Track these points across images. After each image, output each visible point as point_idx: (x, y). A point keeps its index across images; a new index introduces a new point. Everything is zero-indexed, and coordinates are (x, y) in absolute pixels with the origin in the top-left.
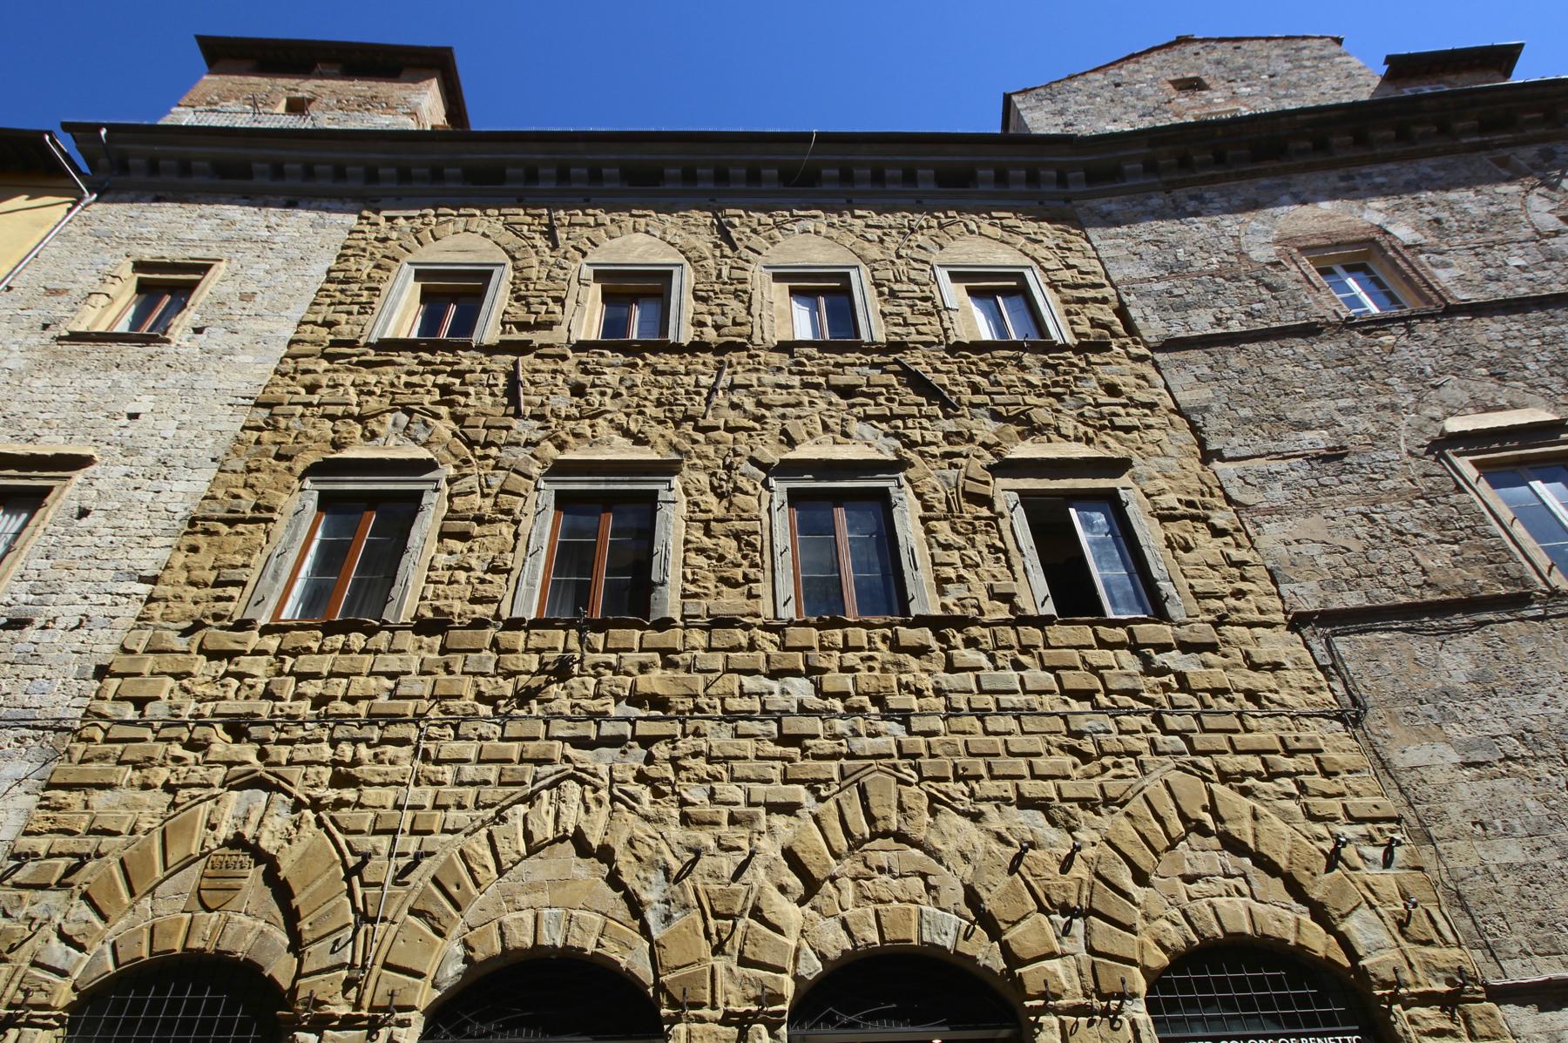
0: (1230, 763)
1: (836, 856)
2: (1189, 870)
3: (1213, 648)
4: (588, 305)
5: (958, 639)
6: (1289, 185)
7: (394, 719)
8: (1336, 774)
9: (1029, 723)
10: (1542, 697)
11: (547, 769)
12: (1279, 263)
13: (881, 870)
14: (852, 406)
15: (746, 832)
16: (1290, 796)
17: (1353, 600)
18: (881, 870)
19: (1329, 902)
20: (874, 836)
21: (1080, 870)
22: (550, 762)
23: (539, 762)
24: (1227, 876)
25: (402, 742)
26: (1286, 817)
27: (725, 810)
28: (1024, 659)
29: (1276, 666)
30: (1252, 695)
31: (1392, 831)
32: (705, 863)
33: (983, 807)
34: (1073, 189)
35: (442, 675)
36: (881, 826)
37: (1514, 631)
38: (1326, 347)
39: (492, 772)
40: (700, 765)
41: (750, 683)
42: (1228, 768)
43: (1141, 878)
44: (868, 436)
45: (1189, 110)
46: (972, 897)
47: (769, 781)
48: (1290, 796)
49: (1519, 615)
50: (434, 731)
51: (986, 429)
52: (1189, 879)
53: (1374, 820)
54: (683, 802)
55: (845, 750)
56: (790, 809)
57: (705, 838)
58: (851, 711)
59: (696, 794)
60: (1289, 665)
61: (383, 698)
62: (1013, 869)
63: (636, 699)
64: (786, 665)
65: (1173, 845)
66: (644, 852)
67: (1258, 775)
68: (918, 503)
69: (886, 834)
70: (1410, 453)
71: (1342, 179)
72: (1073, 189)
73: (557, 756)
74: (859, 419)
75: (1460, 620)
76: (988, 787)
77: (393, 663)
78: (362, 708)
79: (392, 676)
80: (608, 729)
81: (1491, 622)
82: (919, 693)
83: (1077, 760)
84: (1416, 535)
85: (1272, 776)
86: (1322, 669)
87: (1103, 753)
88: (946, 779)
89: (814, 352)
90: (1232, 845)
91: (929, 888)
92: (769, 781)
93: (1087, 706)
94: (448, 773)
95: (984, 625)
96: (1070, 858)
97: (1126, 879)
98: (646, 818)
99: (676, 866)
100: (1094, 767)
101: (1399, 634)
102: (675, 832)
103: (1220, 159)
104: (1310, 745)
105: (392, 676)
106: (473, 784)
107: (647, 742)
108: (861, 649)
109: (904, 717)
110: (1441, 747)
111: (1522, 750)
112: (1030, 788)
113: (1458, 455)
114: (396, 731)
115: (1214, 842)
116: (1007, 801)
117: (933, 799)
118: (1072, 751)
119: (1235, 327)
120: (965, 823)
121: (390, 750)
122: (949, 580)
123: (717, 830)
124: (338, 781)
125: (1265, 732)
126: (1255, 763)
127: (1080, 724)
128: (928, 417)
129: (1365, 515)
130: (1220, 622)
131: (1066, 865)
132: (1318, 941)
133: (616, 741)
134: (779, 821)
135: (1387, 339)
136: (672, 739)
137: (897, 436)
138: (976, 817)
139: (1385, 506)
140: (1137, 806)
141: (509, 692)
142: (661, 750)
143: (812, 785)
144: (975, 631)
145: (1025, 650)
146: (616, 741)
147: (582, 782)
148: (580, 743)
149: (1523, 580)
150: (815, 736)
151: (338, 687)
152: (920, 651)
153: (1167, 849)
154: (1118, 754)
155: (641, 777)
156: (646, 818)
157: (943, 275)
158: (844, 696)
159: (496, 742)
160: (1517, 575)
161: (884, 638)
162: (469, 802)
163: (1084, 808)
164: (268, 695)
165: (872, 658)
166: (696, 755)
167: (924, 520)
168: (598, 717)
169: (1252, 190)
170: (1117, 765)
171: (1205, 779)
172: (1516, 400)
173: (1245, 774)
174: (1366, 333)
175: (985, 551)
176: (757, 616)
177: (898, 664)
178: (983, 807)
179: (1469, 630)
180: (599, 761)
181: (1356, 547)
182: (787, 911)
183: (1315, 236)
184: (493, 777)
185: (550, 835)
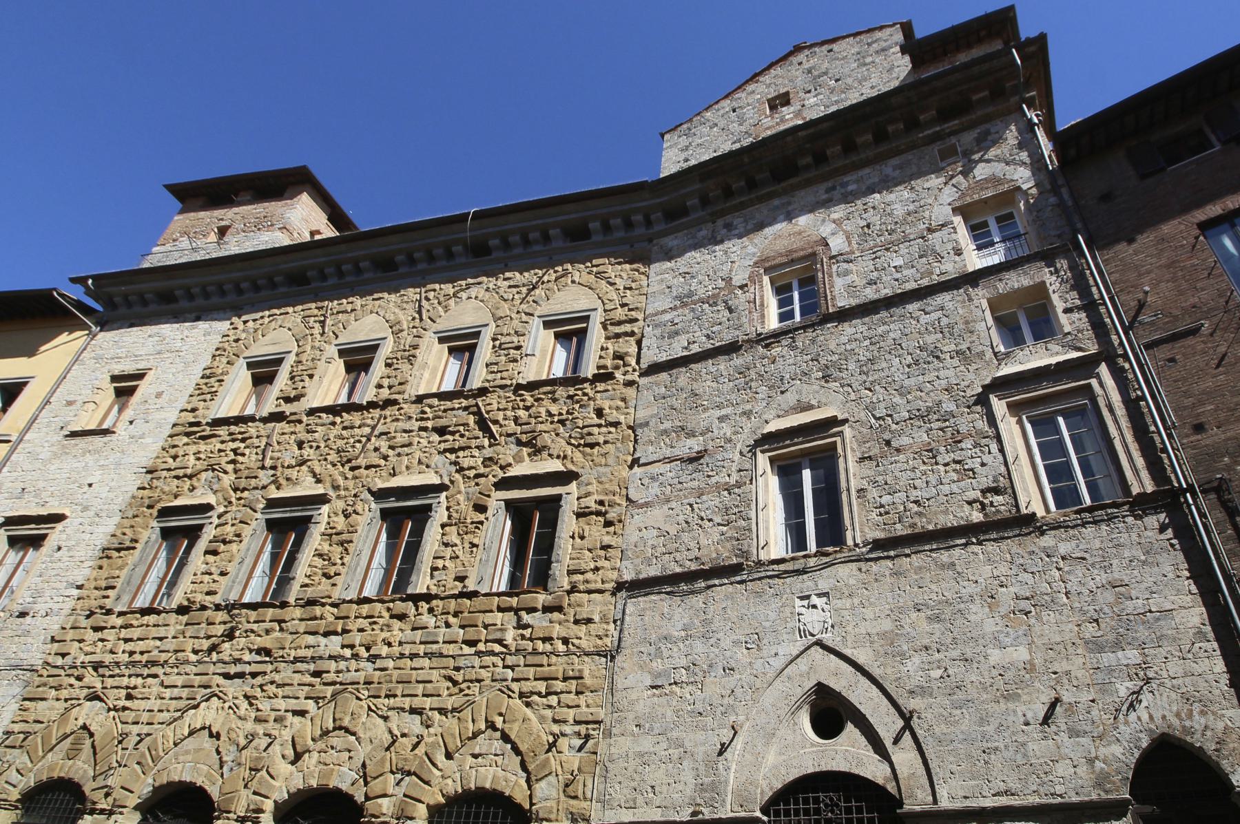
0: (527, 686)
1: (313, 740)
2: (477, 751)
3: (559, 609)
4: (326, 381)
5: (424, 606)
6: (789, 203)
7: (154, 663)
8: (582, 693)
9: (436, 662)
10: (712, 641)
11: (208, 691)
12: (746, 285)
13: (332, 748)
14: (440, 442)
15: (277, 726)
16: (550, 707)
17: (653, 571)
18: (332, 748)
19: (533, 773)
20: (335, 729)
21: (420, 750)
22: (209, 687)
23: (206, 687)
24: (496, 755)
25: (155, 676)
26: (542, 719)
27: (273, 714)
28: (452, 620)
29: (589, 621)
30: (565, 641)
31: (594, 730)
32: (256, 741)
33: (389, 713)
34: (657, 228)
35: (182, 639)
36: (338, 723)
37: (723, 591)
38: (738, 360)
39: (185, 693)
40: (271, 689)
41: (310, 639)
42: (525, 689)
43: (449, 756)
44: (440, 465)
45: (772, 125)
46: (364, 765)
47: (297, 698)
48: (550, 707)
49: (738, 578)
50: (168, 670)
51: (507, 452)
52: (475, 756)
53: (587, 723)
54: (258, 710)
55: (338, 680)
56: (301, 713)
57: (260, 729)
58: (356, 656)
59: (264, 705)
60: (596, 618)
61: (155, 652)
62: (388, 749)
63: (258, 652)
64: (331, 629)
65: (475, 735)
66: (233, 735)
67: (539, 694)
68: (446, 513)
69: (340, 728)
70: (741, 453)
71: (827, 191)
72: (657, 228)
73: (214, 684)
74: (439, 453)
75: (702, 584)
76: (398, 702)
77: (161, 632)
78: (145, 658)
79: (161, 639)
80: (239, 668)
81: (715, 586)
82: (389, 645)
83: (450, 685)
84: (710, 520)
85: (548, 694)
86: (615, 622)
87: (465, 681)
88: (379, 697)
89: (435, 401)
90: (506, 738)
91: (350, 758)
92: (297, 698)
93: (473, 650)
94: (168, 693)
95: (442, 599)
96: (418, 743)
97: (440, 758)
98: (240, 718)
99: (243, 742)
100: (456, 690)
101: (663, 596)
102: (250, 726)
103: (752, 185)
104: (577, 674)
105: (161, 639)
106: (176, 699)
107: (254, 675)
108: (372, 617)
109: (373, 658)
110: (646, 674)
111: (684, 679)
112: (417, 702)
113: (763, 452)
114: (154, 670)
115: (498, 734)
116: (403, 709)
117: (370, 709)
118: (450, 679)
119: (695, 349)
120: (380, 721)
121: (150, 680)
122: (436, 569)
123: (266, 725)
124: (129, 697)
125: (559, 666)
126: (541, 687)
127: (461, 662)
128: (477, 447)
129: (691, 505)
130: (573, 590)
131: (415, 746)
132: (520, 796)
133: (241, 675)
134: (297, 719)
135: (776, 350)
136: (265, 673)
137: (456, 463)
138: (386, 718)
139: (704, 498)
140: (467, 714)
141: (205, 648)
142: (259, 680)
143: (316, 699)
144: (434, 602)
145: (456, 615)
146: (241, 675)
147: (220, 698)
148: (227, 676)
149: (745, 554)
150: (328, 672)
151: (141, 646)
152: (402, 617)
153: (469, 739)
154: (471, 681)
155: (246, 697)
156: (240, 718)
157: (536, 323)
158: (352, 647)
159: (192, 676)
160: (745, 548)
161: (389, 609)
162: (172, 709)
163: (440, 713)
164: (112, 652)
165: (375, 623)
166: (272, 683)
167: (443, 526)
168: (237, 661)
169: (765, 212)
170: (469, 688)
171: (509, 697)
172: (824, 400)
173: (532, 693)
174: (767, 346)
175: (467, 545)
176: (330, 597)
177: (388, 626)
178: (389, 713)
179: (700, 592)
180: (233, 689)
181: (673, 532)
182: (283, 768)
183: (781, 255)
184: (184, 696)
185: (198, 727)
